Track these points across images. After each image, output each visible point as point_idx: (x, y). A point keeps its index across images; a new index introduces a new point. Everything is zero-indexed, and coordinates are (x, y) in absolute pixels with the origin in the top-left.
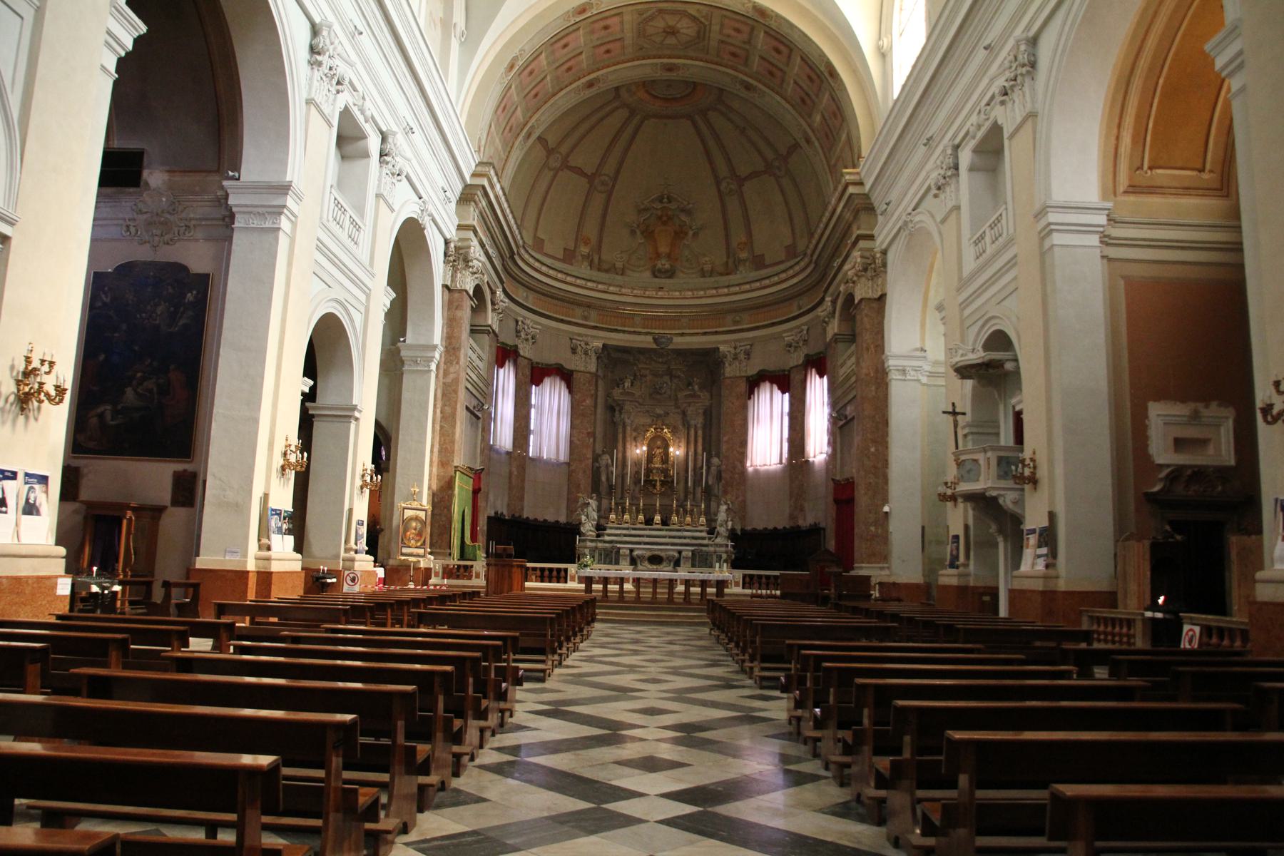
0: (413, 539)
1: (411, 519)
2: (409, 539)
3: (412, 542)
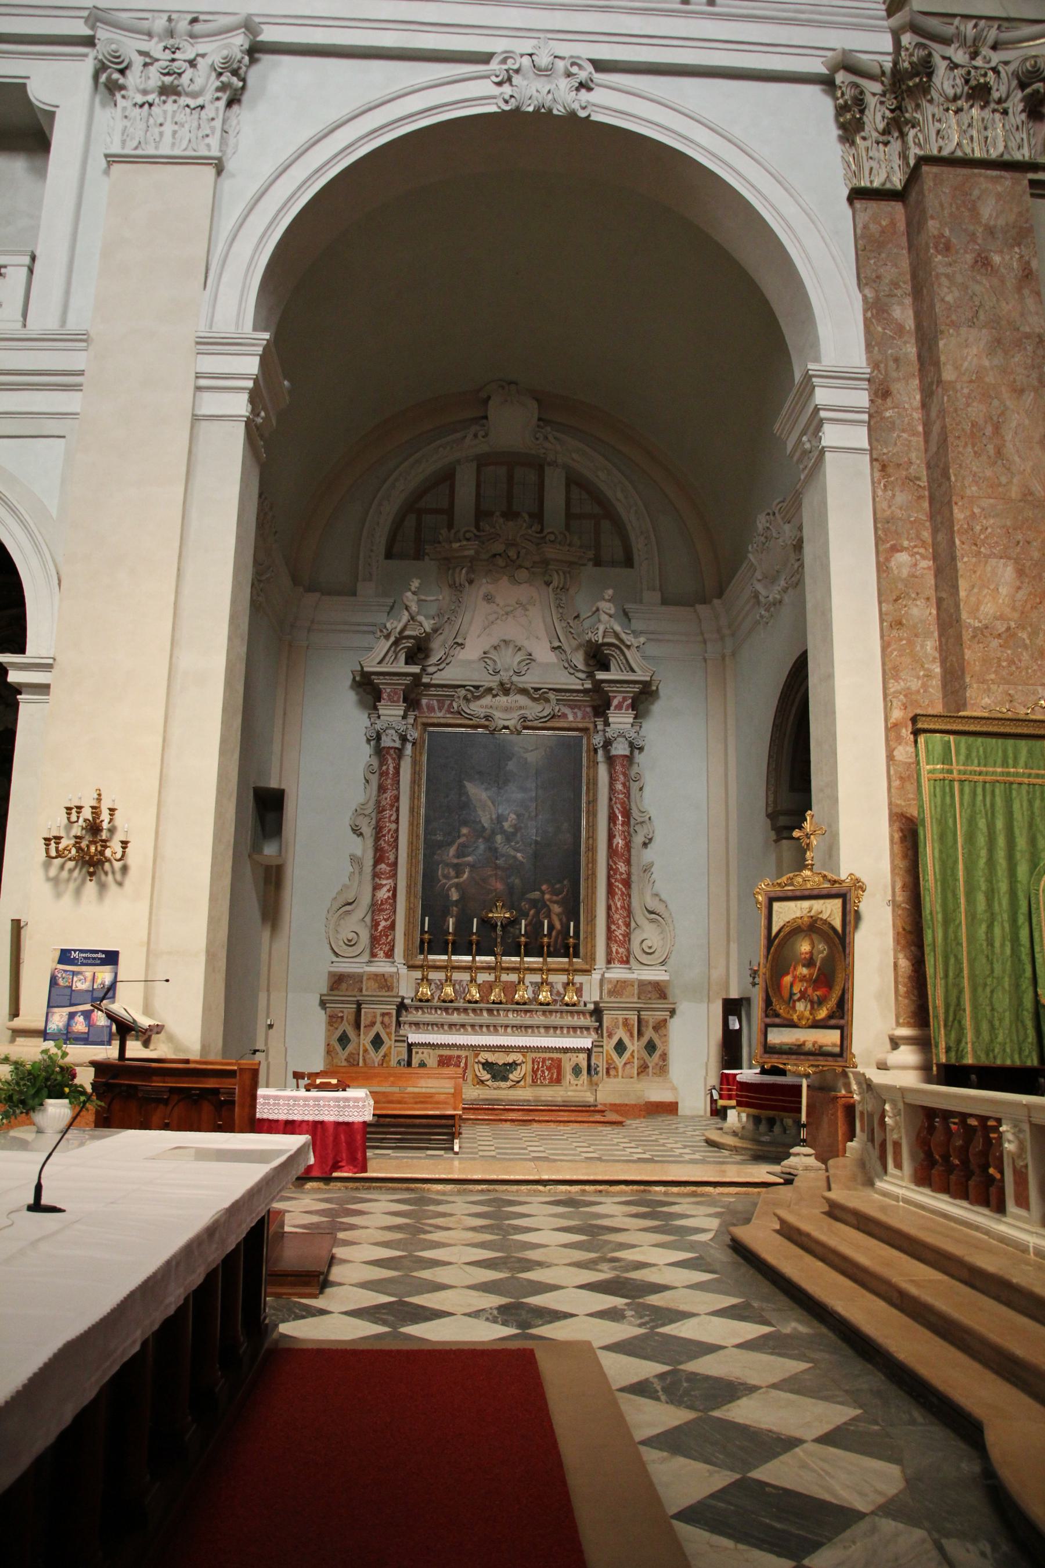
0: (803, 996)
1: (796, 930)
2: (790, 1001)
3: (800, 1006)
